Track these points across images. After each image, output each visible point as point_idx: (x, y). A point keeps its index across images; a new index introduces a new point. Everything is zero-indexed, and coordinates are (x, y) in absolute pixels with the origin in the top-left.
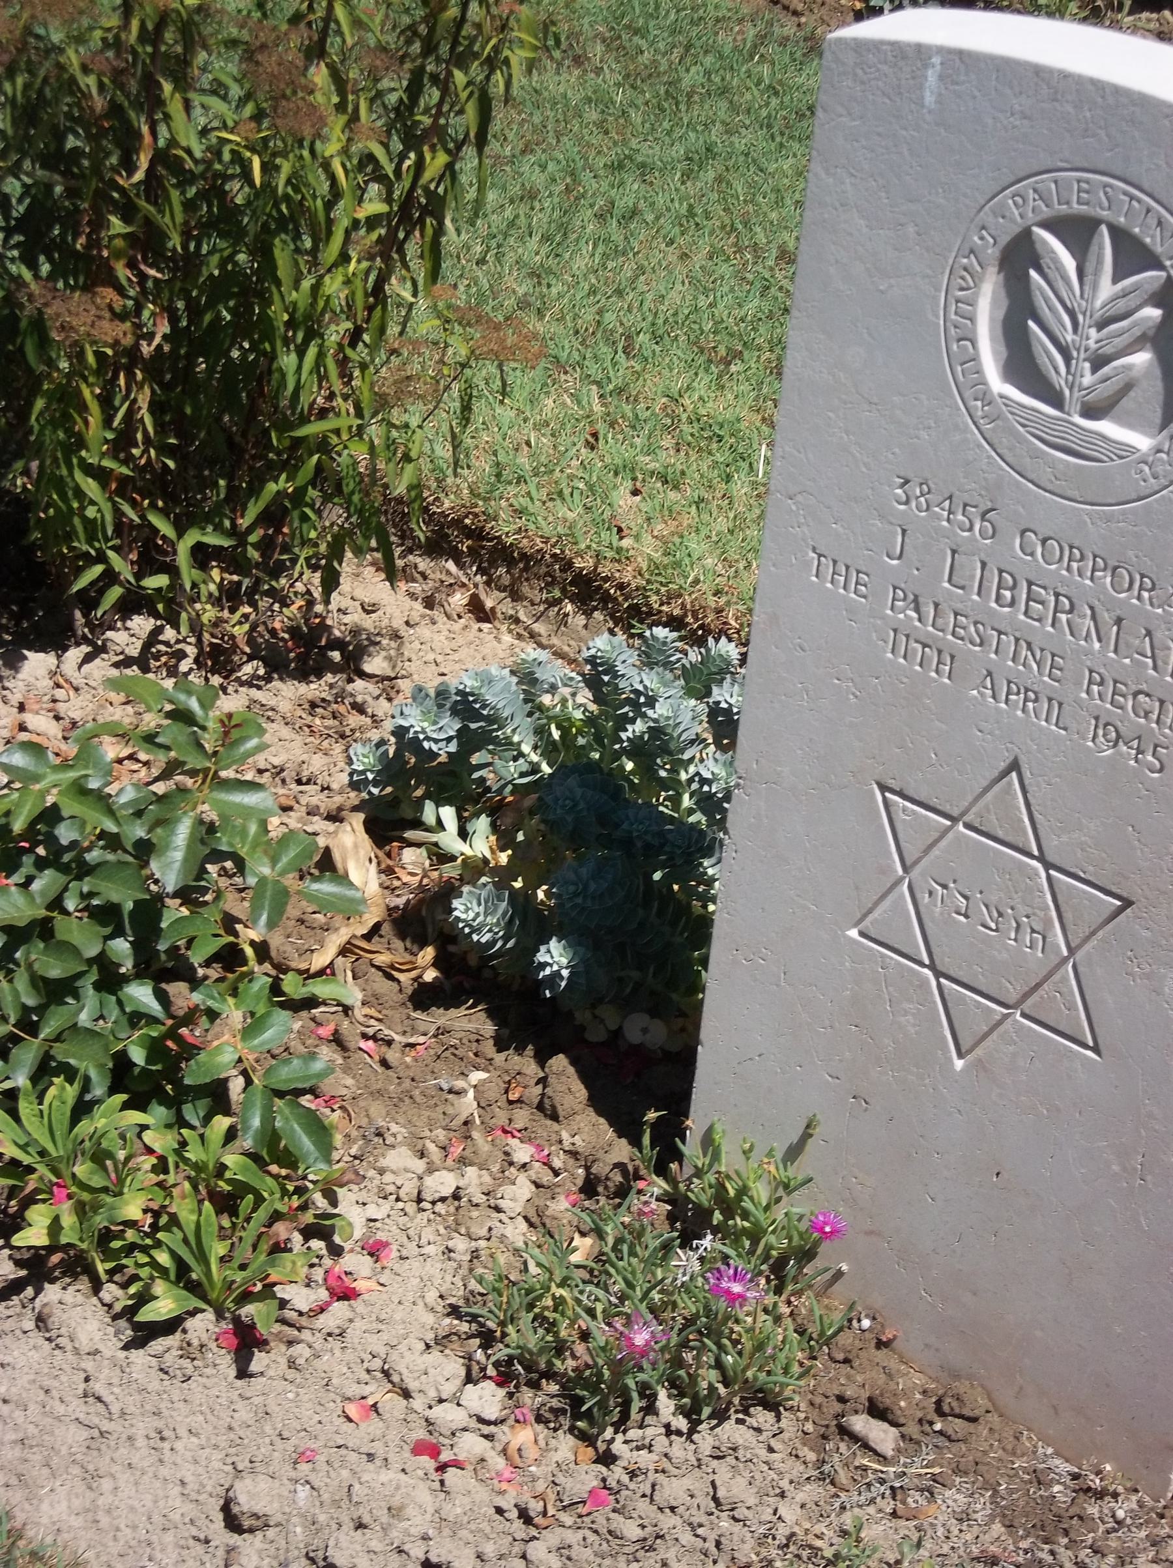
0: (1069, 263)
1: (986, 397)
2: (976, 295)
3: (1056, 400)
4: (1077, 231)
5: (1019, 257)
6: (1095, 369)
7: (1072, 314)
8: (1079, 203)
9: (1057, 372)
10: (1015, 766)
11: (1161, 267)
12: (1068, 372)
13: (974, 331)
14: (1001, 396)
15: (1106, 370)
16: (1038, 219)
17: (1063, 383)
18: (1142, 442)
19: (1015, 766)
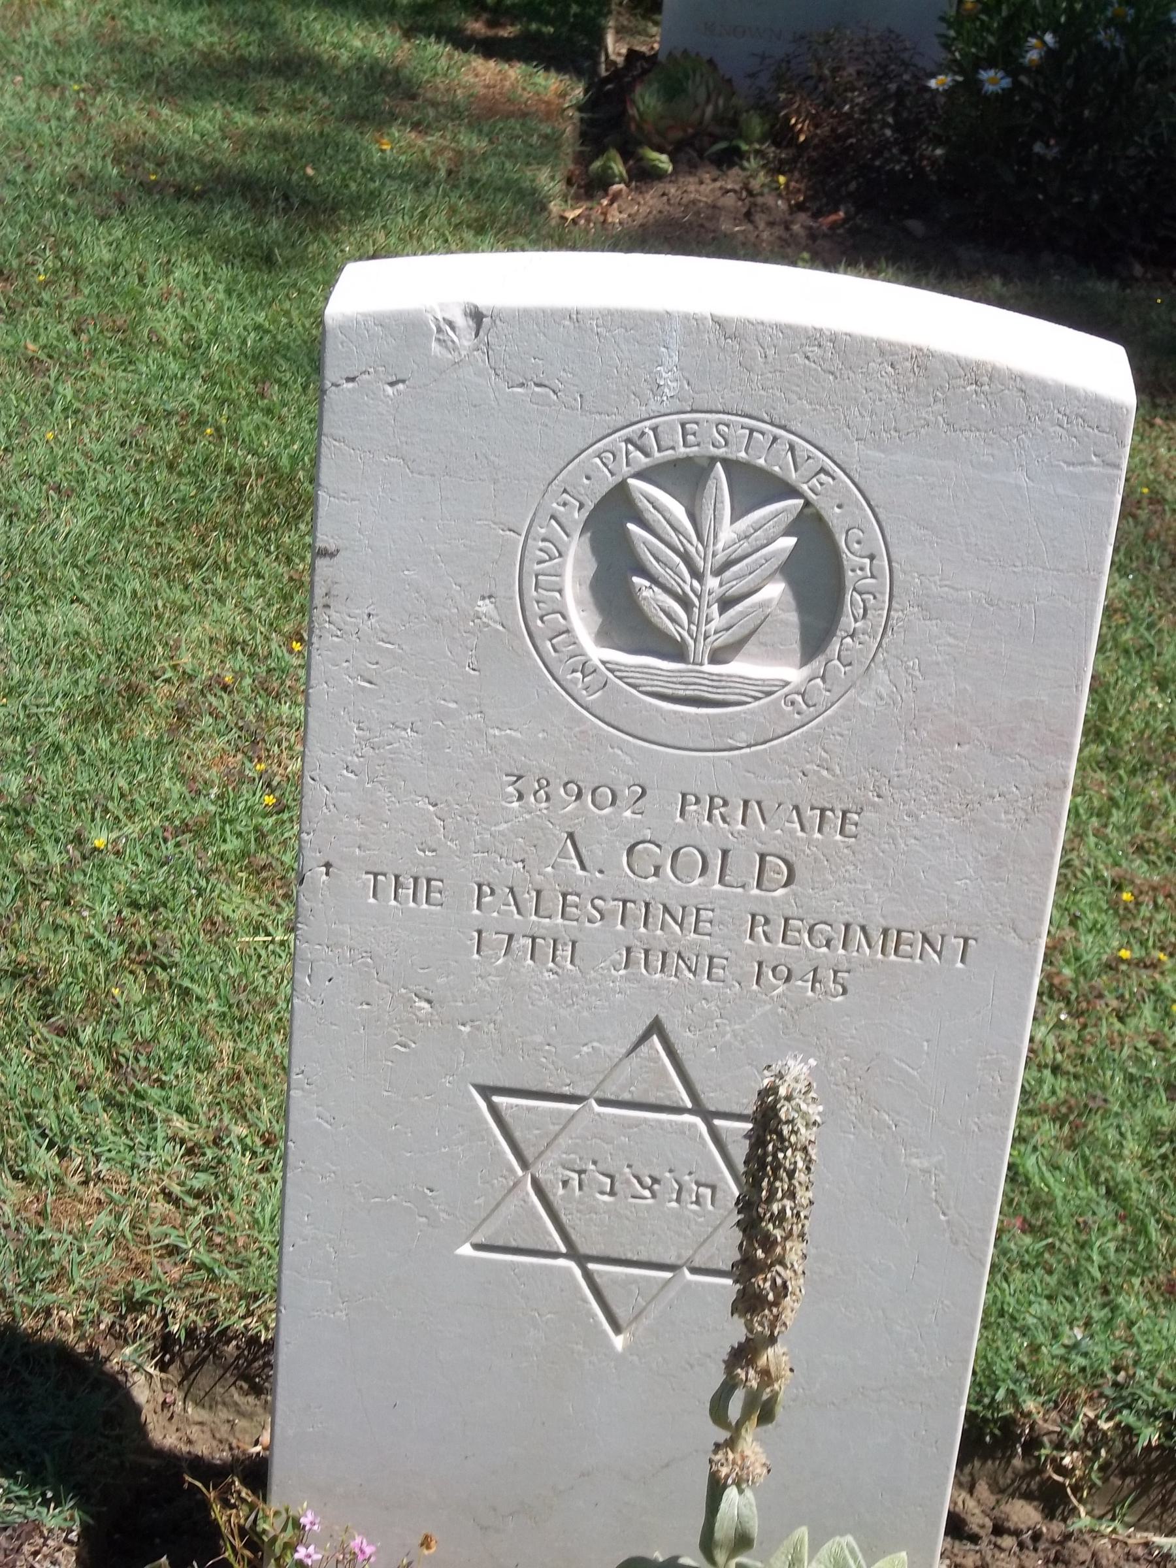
0: (678, 510)
1: (585, 668)
2: (562, 565)
3: (676, 651)
4: (686, 476)
5: (613, 515)
6: (722, 611)
8: (685, 445)
10: (656, 1027)
11: (794, 492)
12: (690, 622)
13: (564, 605)
14: (603, 663)
15: (732, 612)
17: (685, 634)
19: (656, 1027)
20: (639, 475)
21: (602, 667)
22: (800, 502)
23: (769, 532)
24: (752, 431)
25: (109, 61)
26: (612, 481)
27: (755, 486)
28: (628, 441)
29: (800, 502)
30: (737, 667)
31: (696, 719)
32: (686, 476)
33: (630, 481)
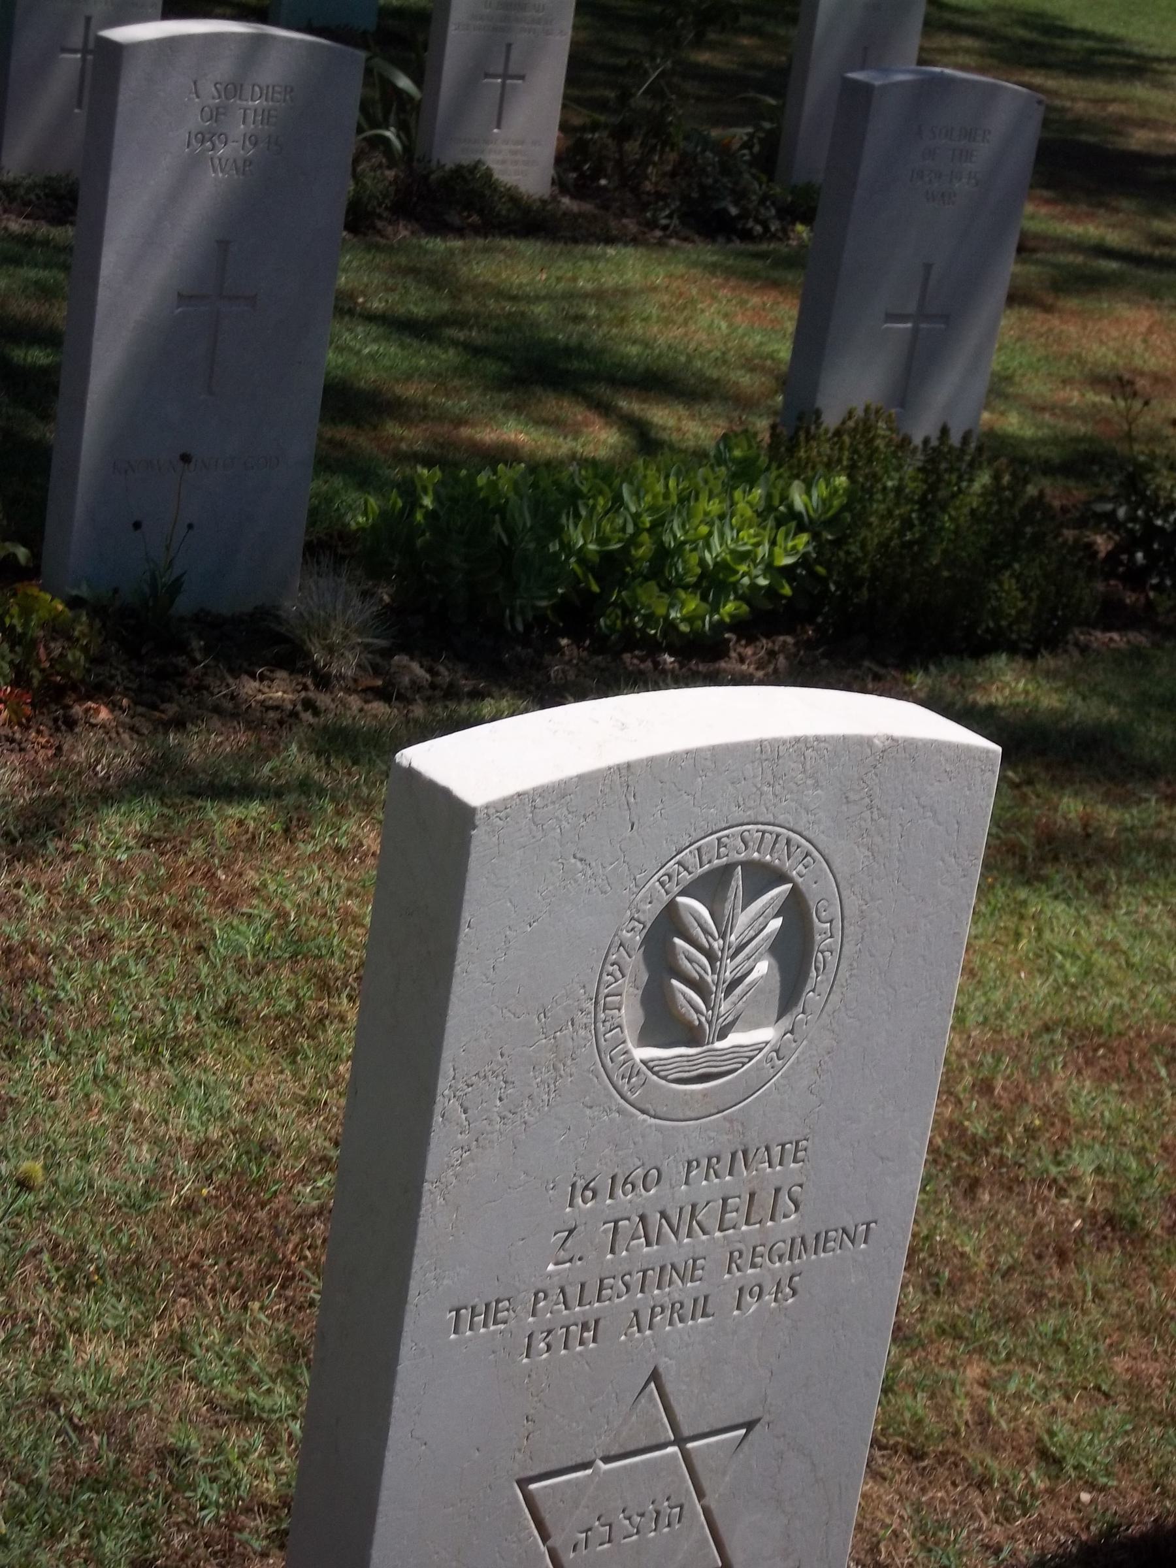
4: (711, 886)
7: (709, 954)
9: (697, 1011)
10: (655, 1376)
14: (644, 1062)
16: (680, 888)
18: (766, 1034)
19: (655, 1376)
20: (683, 893)
21: (644, 1068)
22: (790, 886)
23: (759, 917)
24: (764, 832)
25: (919, 492)
26: (667, 899)
27: (762, 877)
28: (679, 863)
29: (790, 886)
30: (735, 1039)
31: (705, 1094)
32: (711, 886)
33: (680, 899)
